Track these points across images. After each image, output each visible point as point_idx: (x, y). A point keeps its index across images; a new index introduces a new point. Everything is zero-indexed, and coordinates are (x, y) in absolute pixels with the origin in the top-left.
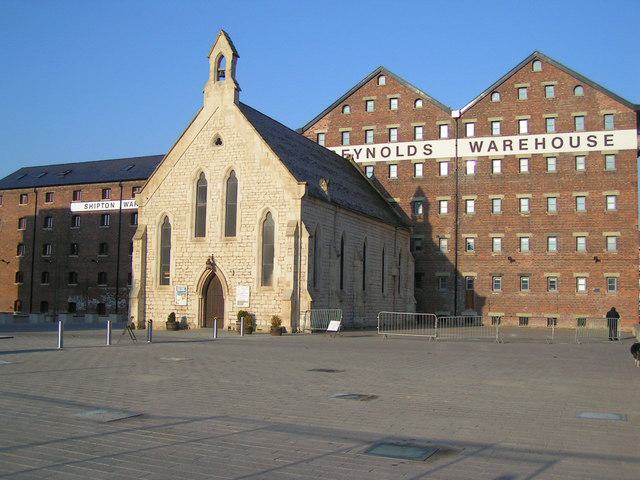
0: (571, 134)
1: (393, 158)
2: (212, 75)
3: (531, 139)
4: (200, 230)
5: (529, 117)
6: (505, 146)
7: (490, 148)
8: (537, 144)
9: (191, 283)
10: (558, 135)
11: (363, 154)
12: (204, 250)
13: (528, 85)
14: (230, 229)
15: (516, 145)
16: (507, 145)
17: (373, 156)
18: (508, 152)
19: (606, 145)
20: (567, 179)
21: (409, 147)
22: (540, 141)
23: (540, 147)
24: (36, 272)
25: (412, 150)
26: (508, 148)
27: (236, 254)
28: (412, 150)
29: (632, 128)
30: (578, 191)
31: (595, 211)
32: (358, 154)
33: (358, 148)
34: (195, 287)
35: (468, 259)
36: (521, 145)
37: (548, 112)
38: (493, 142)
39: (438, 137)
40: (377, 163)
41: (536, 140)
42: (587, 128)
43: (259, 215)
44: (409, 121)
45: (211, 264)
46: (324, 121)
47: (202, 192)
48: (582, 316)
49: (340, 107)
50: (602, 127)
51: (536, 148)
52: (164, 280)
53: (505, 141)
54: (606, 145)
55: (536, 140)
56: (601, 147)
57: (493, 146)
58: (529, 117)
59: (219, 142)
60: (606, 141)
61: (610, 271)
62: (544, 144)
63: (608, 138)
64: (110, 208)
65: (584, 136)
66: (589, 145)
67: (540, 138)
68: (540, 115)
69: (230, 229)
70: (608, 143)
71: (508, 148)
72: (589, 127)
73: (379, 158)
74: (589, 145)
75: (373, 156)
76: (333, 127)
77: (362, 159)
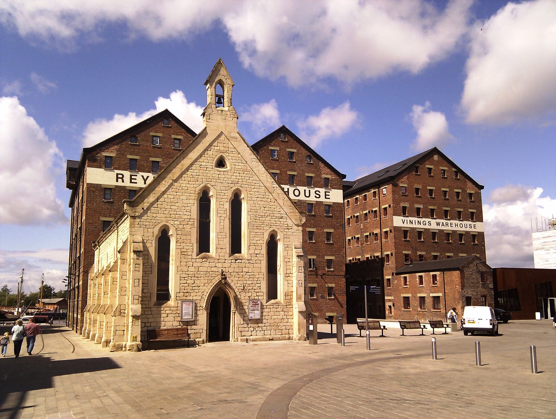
0: (306, 188)
5: (278, 172)
10: (298, 187)
12: (213, 264)
14: (236, 247)
19: (326, 198)
27: (245, 270)
29: (341, 190)
30: (310, 227)
37: (291, 170)
43: (266, 237)
54: (326, 198)
56: (323, 199)
60: (326, 195)
66: (315, 197)
68: (286, 172)
69: (236, 247)
70: (327, 197)
72: (316, 185)
74: (315, 197)
76: (121, 154)
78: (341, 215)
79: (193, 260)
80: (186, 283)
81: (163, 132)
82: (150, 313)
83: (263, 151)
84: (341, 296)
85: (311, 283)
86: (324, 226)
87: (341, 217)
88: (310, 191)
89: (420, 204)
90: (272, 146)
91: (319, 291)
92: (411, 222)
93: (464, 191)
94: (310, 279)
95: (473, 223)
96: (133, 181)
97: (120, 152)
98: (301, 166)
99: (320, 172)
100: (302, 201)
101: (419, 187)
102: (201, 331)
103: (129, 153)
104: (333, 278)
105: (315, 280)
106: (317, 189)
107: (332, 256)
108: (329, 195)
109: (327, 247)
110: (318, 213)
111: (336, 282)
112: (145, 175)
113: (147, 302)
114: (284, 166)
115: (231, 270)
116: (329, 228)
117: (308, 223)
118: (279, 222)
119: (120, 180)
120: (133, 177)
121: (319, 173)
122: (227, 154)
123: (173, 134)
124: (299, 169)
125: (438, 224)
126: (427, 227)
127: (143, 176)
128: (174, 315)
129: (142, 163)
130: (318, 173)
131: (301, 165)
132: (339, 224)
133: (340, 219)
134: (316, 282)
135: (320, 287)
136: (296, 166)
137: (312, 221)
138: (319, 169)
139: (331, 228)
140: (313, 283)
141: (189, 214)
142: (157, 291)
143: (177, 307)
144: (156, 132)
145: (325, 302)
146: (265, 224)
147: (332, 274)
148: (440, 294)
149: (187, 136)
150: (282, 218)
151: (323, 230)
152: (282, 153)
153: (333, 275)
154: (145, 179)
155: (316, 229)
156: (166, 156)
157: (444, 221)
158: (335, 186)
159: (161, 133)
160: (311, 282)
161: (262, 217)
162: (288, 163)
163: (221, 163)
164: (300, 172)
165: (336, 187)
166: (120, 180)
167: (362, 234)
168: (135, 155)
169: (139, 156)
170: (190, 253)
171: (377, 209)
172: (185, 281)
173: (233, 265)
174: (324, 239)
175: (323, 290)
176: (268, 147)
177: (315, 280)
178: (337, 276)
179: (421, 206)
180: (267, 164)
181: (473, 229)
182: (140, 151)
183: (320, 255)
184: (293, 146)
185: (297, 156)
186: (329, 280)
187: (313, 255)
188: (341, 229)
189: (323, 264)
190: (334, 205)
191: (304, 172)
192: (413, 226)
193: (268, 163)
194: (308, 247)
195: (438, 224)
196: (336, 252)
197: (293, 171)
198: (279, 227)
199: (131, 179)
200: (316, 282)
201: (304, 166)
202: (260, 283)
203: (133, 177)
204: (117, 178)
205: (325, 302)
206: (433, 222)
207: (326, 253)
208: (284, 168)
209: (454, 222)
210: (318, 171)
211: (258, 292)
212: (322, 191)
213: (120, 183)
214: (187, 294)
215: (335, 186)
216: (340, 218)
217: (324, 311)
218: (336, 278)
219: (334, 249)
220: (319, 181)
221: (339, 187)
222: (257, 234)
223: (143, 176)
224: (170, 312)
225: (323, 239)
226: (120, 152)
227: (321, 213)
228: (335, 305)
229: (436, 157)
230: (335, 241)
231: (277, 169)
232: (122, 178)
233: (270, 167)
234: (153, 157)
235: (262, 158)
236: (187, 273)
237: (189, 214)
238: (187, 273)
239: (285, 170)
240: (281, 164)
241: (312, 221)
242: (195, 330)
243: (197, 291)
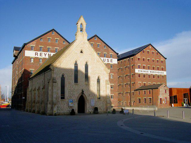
2: (79, 30)
13: (94, 43)
32: (45, 55)
34: (76, 100)
43: (97, 78)
45: (83, 92)
46: (35, 42)
52: (63, 98)
56: (110, 62)
59: (81, 52)
65: (106, 59)
79: (73, 86)
89: (144, 64)
92: (141, 71)
93: (160, 60)
95: (162, 72)
96: (41, 55)
101: (145, 58)
106: (108, 58)
112: (45, 53)
113: (58, 100)
115: (85, 89)
119: (36, 55)
120: (41, 54)
125: (151, 72)
126: (147, 73)
129: (44, 49)
142: (61, 96)
148: (151, 98)
150: (102, 71)
157: (153, 71)
163: (81, 52)
166: (36, 55)
167: (123, 75)
171: (129, 66)
173: (86, 88)
179: (145, 65)
181: (162, 74)
192: (142, 72)
195: (151, 72)
199: (40, 54)
203: (41, 54)
204: (36, 54)
206: (149, 71)
209: (156, 71)
212: (110, 59)
213: (36, 56)
229: (150, 47)
232: (37, 54)
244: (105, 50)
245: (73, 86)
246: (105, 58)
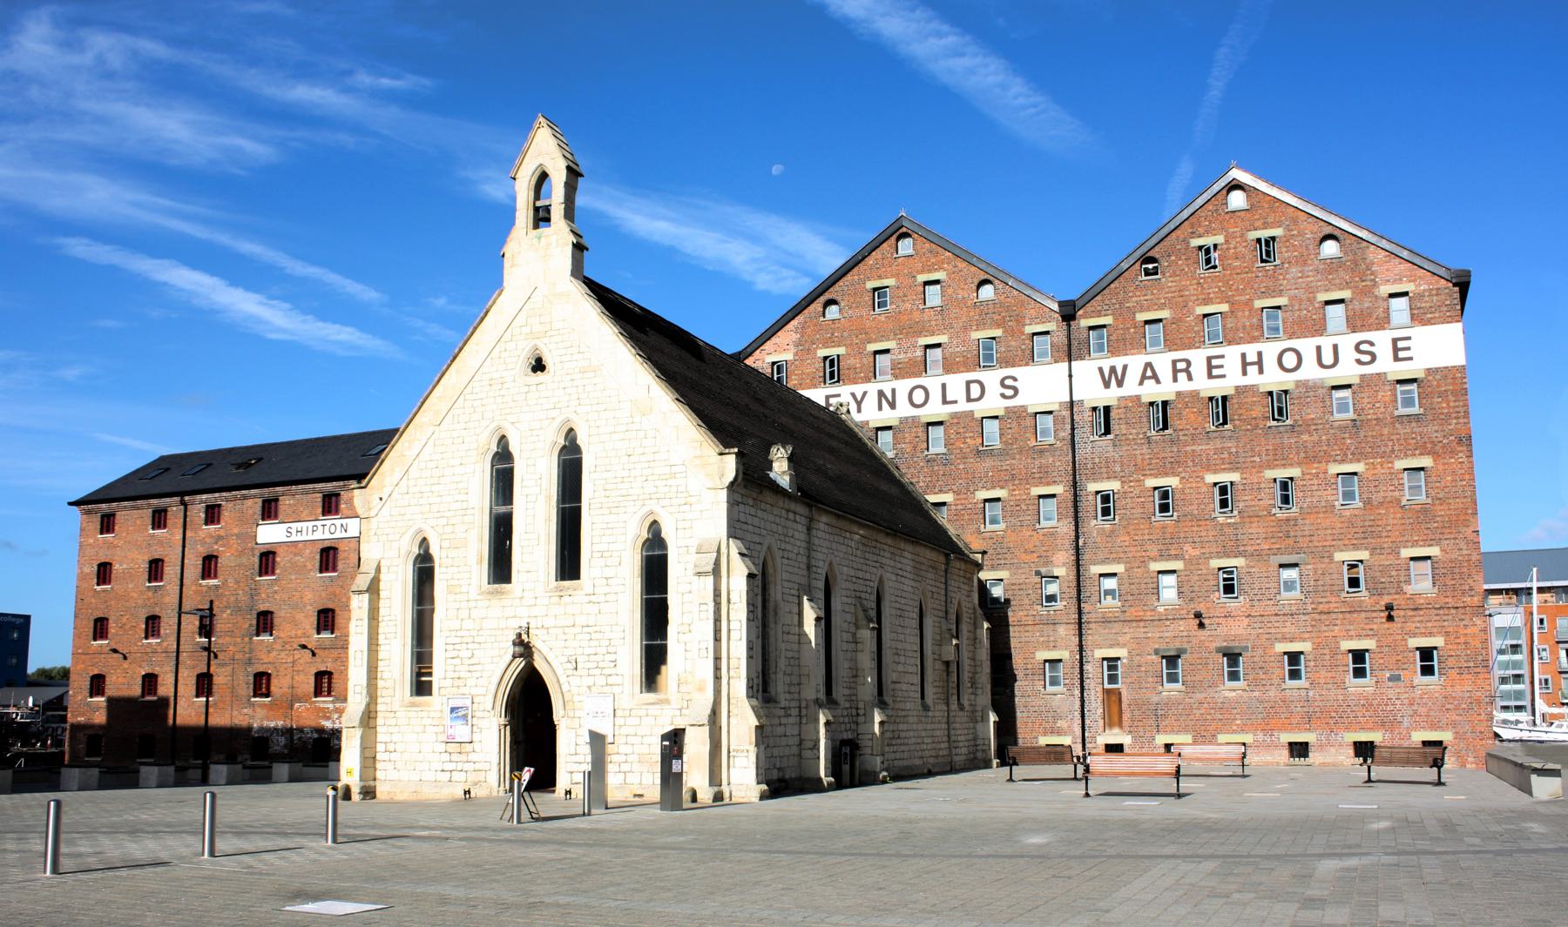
1: (935, 410)
3: (1232, 354)
4: (501, 567)
5: (1224, 308)
6: (1175, 371)
7: (1144, 378)
8: (1245, 364)
9: (483, 691)
11: (871, 402)
14: (569, 564)
15: (1199, 369)
16: (1181, 369)
17: (893, 405)
18: (1183, 384)
19: (1396, 359)
20: (1315, 438)
21: (968, 383)
22: (1252, 357)
23: (1253, 370)
24: (183, 673)
25: (975, 391)
26: (1182, 376)
27: (581, 620)
28: (975, 391)
30: (1343, 461)
31: (1381, 503)
32: (859, 404)
33: (859, 389)
35: (1106, 621)
36: (1210, 367)
38: (1149, 365)
39: (1030, 358)
40: (904, 421)
41: (1243, 356)
42: (1353, 327)
44: (966, 329)
46: (787, 336)
47: (503, 482)
48: (1364, 737)
49: (817, 306)
50: (1383, 322)
51: (1245, 373)
52: (422, 687)
53: (1174, 363)
54: (1396, 359)
55: (1243, 356)
56: (1386, 364)
57: (1150, 373)
58: (1224, 308)
59: (539, 366)
60: (1396, 350)
61: (1424, 635)
62: (1260, 363)
63: (1401, 344)
64: (338, 535)
67: (1251, 351)
68: (1249, 303)
69: (569, 564)
70: (1401, 354)
71: (1182, 376)
72: (1359, 323)
73: (904, 409)
74: (1359, 362)
75: (893, 405)
76: (804, 348)
77: (868, 415)
78: (1458, 407)
79: (471, 604)
80: (458, 657)
81: (896, 276)
82: (393, 722)
83: (1173, 258)
84: (1470, 676)
85: (1351, 638)
86: (1393, 451)
87: (1458, 412)
88: (1335, 347)
90: (1200, 236)
91: (1381, 661)
94: (1348, 627)
97: (801, 348)
98: (1300, 275)
99: (1371, 280)
100: (1310, 383)
102: (487, 766)
103: (820, 345)
104: (1438, 618)
105: (1366, 627)
107: (1429, 546)
108: (1408, 349)
109: (1409, 518)
110: (1372, 411)
111: (1451, 629)
114: (1241, 287)
115: (549, 622)
116: (1415, 455)
117: (1336, 447)
118: (667, 489)
121: (1368, 283)
122: (546, 340)
123: (922, 272)
124: (1294, 287)
127: (853, 395)
128: (436, 729)
129: (851, 361)
130: (1363, 284)
131: (1300, 272)
132: (1452, 438)
133: (1455, 421)
134: (1371, 633)
135: (1387, 649)
136: (1284, 279)
137: (1349, 441)
138: (1369, 272)
139: (1420, 454)
140: (1359, 636)
141: (464, 497)
143: (441, 711)
144: (880, 277)
145: (1407, 695)
146: (630, 498)
147: (1430, 606)
149: (956, 269)
151: (1390, 465)
152: (1235, 248)
153: (1438, 606)
154: (859, 399)
155: (1366, 464)
156: (904, 331)
158: (1429, 316)
159: (892, 276)
160: (1350, 633)
161: (622, 482)
162: (1254, 275)
164: (1300, 293)
165: (1437, 315)
168: (834, 347)
169: (844, 345)
170: (464, 589)
172: (454, 654)
174: (1397, 493)
175: (1399, 658)
176: (1188, 243)
177: (1366, 627)
178: (1453, 611)
180: (1187, 293)
182: (845, 334)
183: (1386, 545)
184: (1270, 220)
185: (1287, 247)
186: (1418, 625)
187: (1356, 547)
188: (1461, 452)
189: (1394, 573)
190: (1431, 378)
191: (1311, 291)
193: (1191, 287)
194: (1339, 525)
196: (1444, 530)
197: (1272, 295)
198: (666, 502)
200: (1371, 633)
201: (1310, 273)
202: (615, 653)
205: (1407, 695)
207: (1405, 539)
208: (1242, 292)
210: (1364, 278)
211: (610, 675)
214: (460, 682)
215: (1429, 316)
216: (1455, 418)
217: (1406, 724)
218: (1445, 618)
219: (1437, 522)
220: (1368, 308)
221: (1448, 314)
222: (609, 526)
223: (853, 395)
224: (429, 721)
225: (1391, 493)
226: (801, 348)
227: (1382, 410)
228: (1448, 706)
230: (1440, 496)
231: (1218, 300)
233: (1198, 300)
234: (876, 341)
235: (1171, 279)
236: (459, 634)
237: (464, 497)
238: (459, 634)
239: (1248, 297)
240: (1231, 283)
241: (1349, 441)
242: (474, 763)
243: (478, 674)
244: (1332, 265)
245: (471, 604)
246: (1335, 340)
